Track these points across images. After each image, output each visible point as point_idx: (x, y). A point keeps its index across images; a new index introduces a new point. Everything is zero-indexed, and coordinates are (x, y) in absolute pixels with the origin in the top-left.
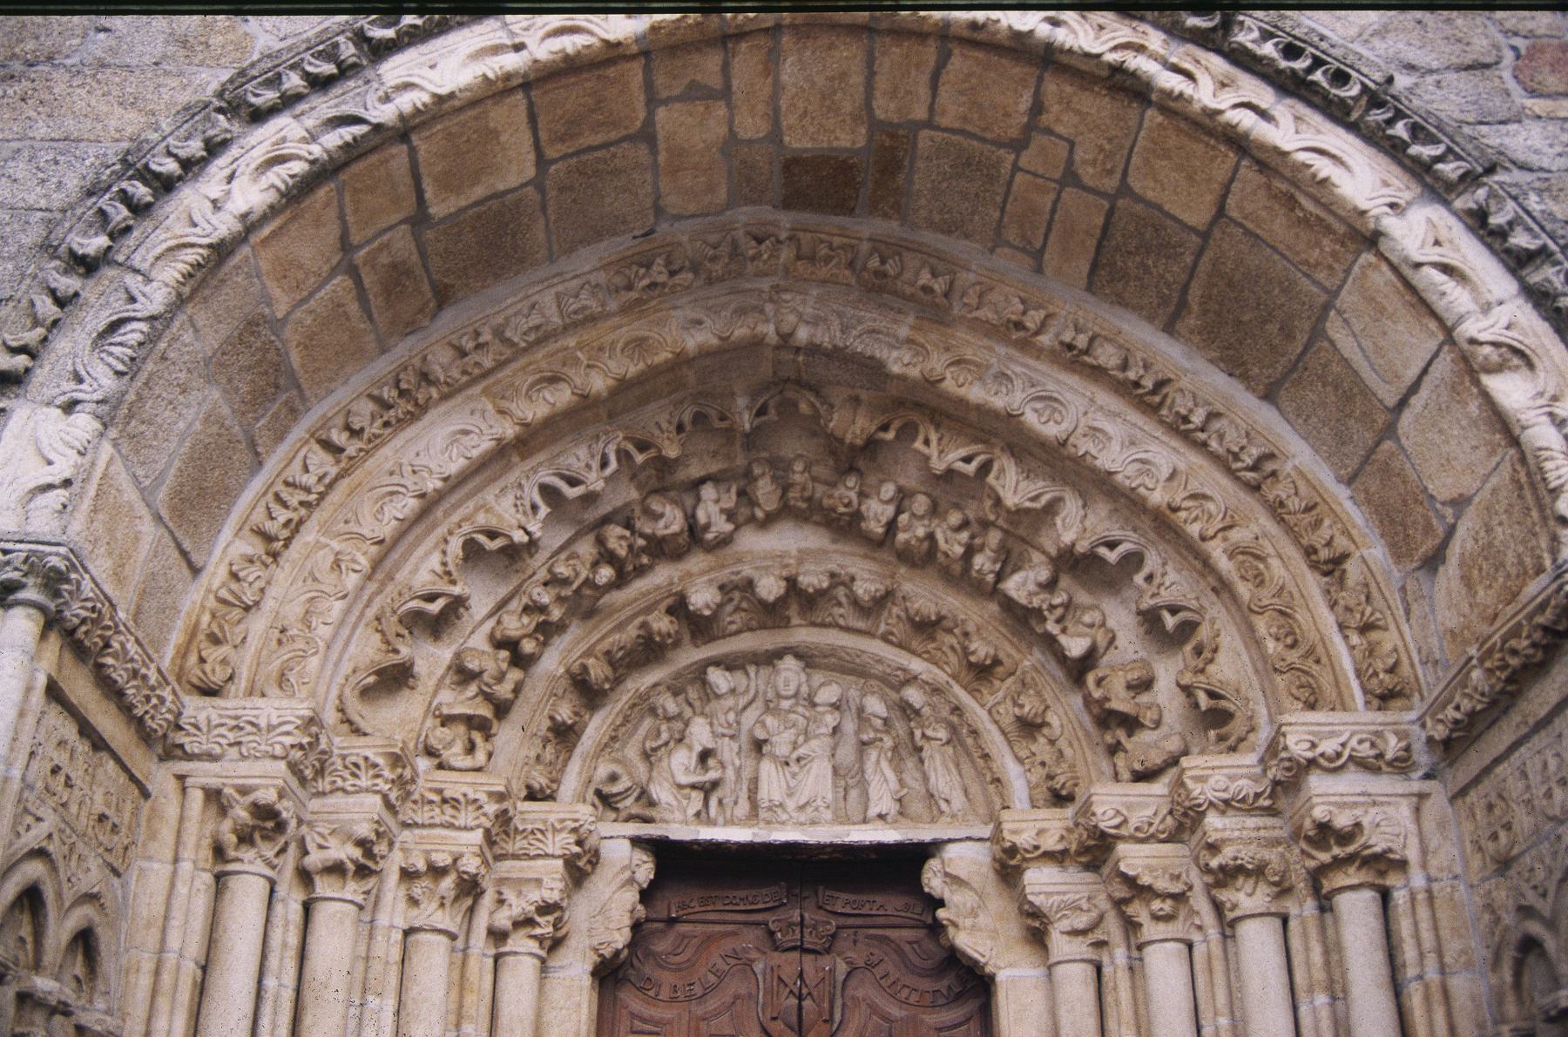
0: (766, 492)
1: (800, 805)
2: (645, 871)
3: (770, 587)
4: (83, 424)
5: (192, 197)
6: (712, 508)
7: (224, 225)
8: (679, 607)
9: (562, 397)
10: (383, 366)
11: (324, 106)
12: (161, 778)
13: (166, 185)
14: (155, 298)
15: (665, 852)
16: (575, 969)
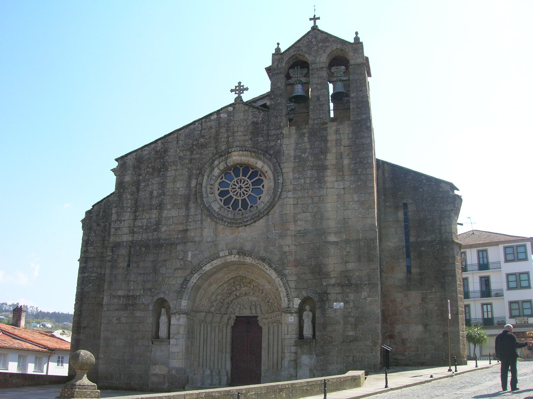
0: (242, 285)
1: (246, 313)
2: (235, 318)
3: (244, 293)
4: (186, 301)
5: (191, 282)
6: (238, 287)
7: (193, 284)
8: (236, 295)
9: (222, 283)
10: (208, 282)
11: (199, 273)
12: (195, 319)
13: (189, 281)
14: (189, 291)
15: (237, 317)
16: (229, 327)
